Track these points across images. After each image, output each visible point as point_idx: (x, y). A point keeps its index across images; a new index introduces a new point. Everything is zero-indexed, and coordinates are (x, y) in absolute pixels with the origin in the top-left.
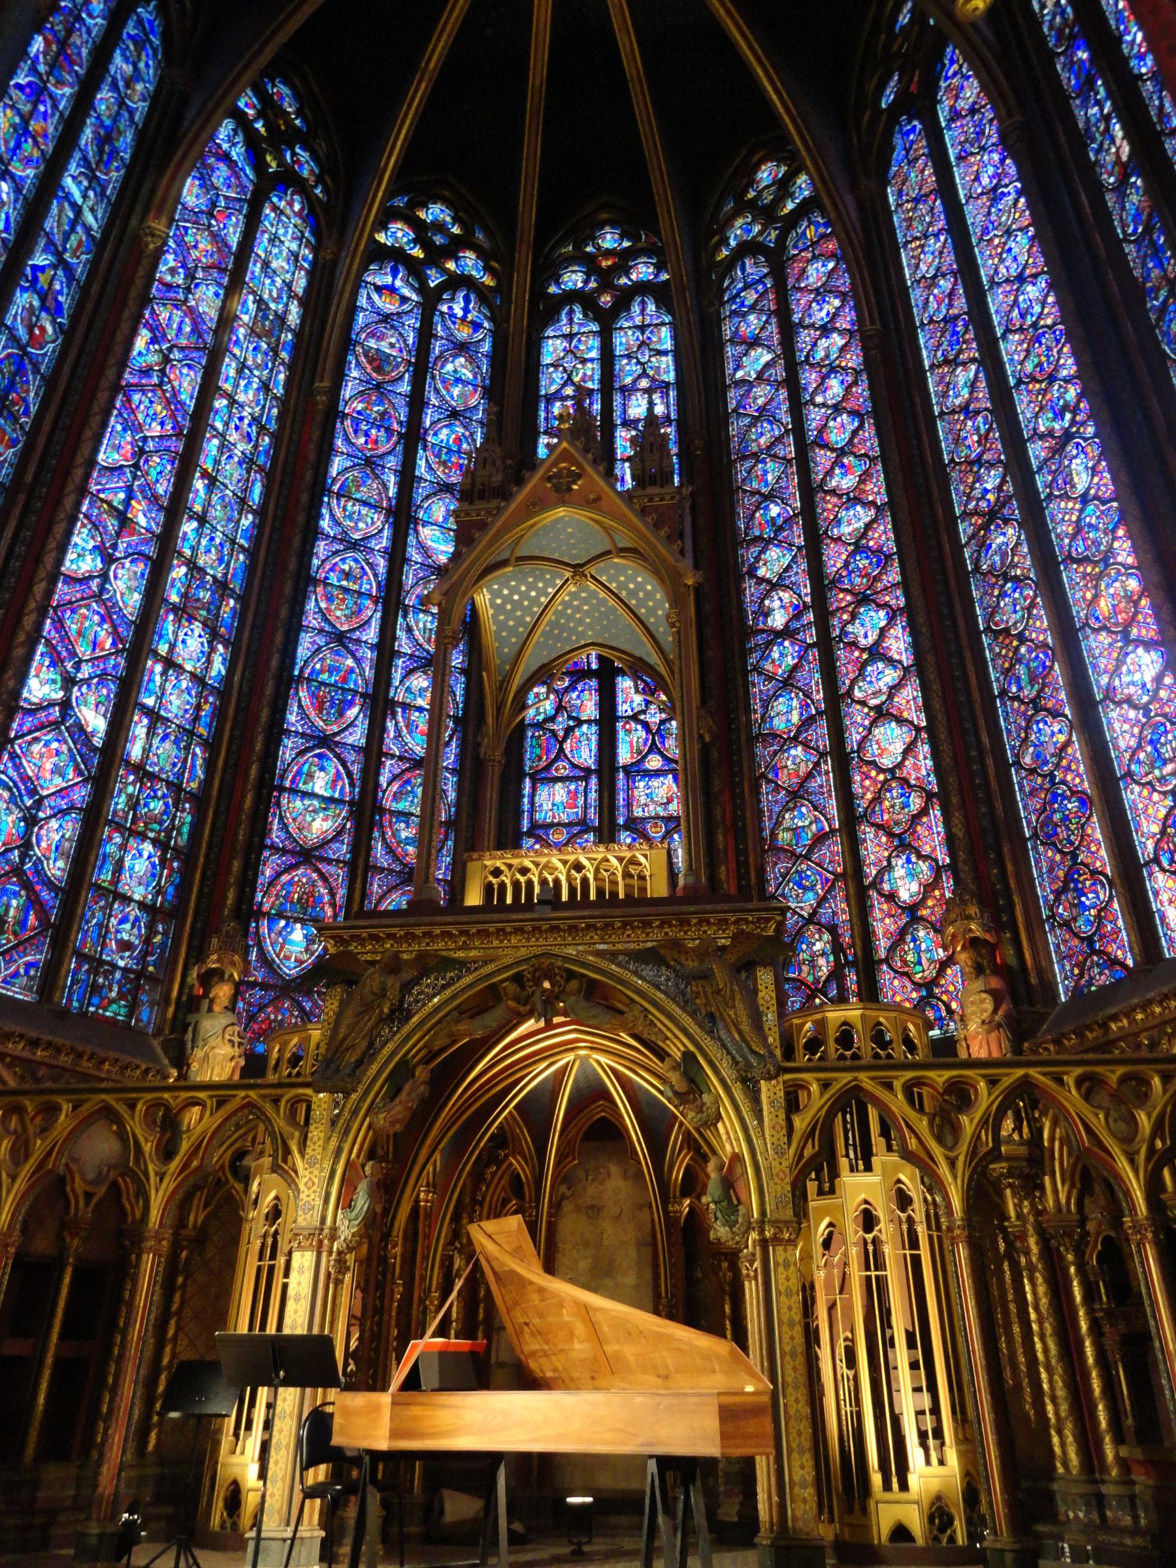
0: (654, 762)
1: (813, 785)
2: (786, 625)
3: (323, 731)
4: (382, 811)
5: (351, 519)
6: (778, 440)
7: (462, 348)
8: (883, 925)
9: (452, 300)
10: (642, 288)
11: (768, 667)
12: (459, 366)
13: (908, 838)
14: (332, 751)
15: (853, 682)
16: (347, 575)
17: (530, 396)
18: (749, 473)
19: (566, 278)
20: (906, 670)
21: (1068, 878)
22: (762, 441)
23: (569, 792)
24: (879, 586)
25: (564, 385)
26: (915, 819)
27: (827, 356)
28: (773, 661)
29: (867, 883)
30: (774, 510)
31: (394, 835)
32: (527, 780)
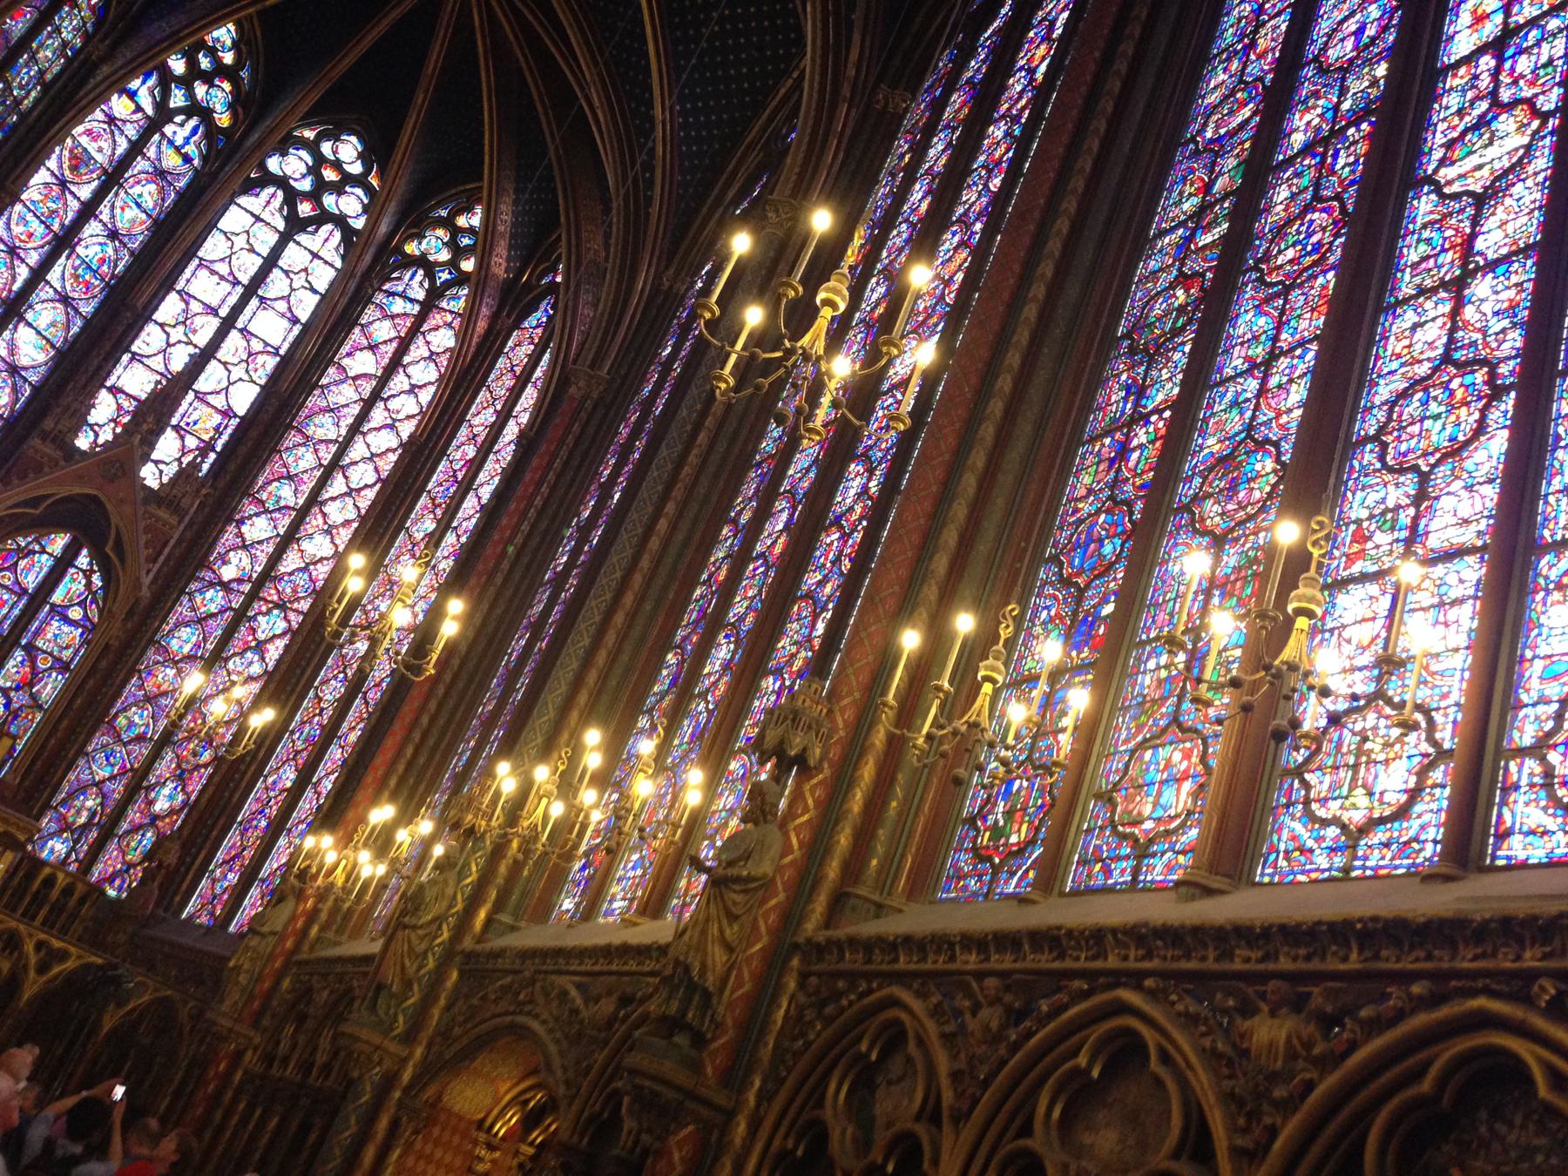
0: (75, 613)
1: (163, 702)
2: (230, 581)
7: (160, 174)
8: (134, 815)
9: (182, 125)
10: (340, 221)
11: (198, 598)
12: (148, 193)
13: (186, 775)
15: (234, 655)
17: (191, 253)
19: (291, 159)
20: (266, 671)
21: (233, 859)
24: (296, 605)
25: (222, 260)
26: (197, 767)
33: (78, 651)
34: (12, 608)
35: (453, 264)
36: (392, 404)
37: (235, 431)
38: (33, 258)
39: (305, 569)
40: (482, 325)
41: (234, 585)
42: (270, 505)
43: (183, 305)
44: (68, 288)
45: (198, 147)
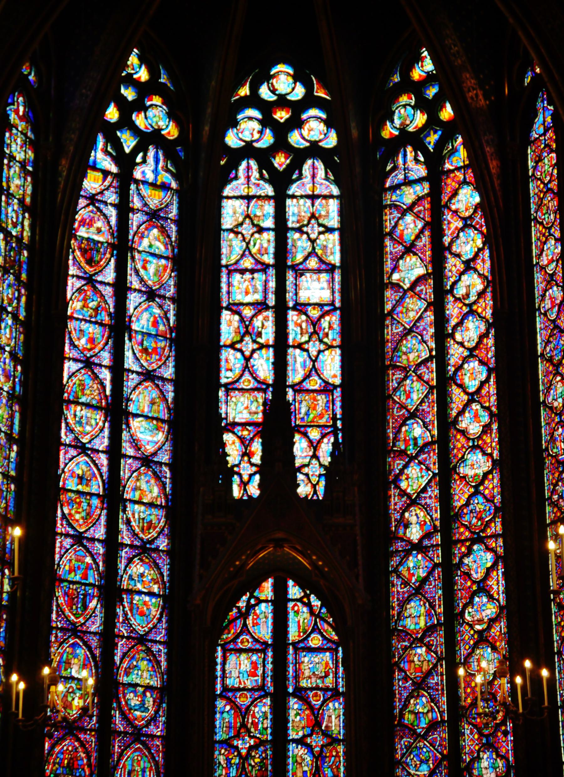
0: (315, 641)
2: (421, 540)
3: (73, 624)
4: (118, 684)
5: (80, 423)
6: (425, 362)
7: (154, 216)
9: (144, 161)
10: (314, 150)
14: (82, 639)
15: (465, 606)
16: (81, 479)
18: (399, 384)
19: (243, 125)
20: (501, 608)
22: (411, 356)
23: (252, 663)
25: (243, 255)
27: (468, 295)
28: (409, 569)
29: (463, 765)
30: (417, 431)
31: (126, 703)
32: (219, 648)
33: (336, 673)
34: (264, 666)
35: (433, 122)
36: (460, 291)
37: (342, 401)
38: (106, 358)
39: (477, 493)
40: (494, 165)
41: (426, 542)
42: (411, 451)
43: (237, 317)
44: (145, 364)
45: (167, 170)
